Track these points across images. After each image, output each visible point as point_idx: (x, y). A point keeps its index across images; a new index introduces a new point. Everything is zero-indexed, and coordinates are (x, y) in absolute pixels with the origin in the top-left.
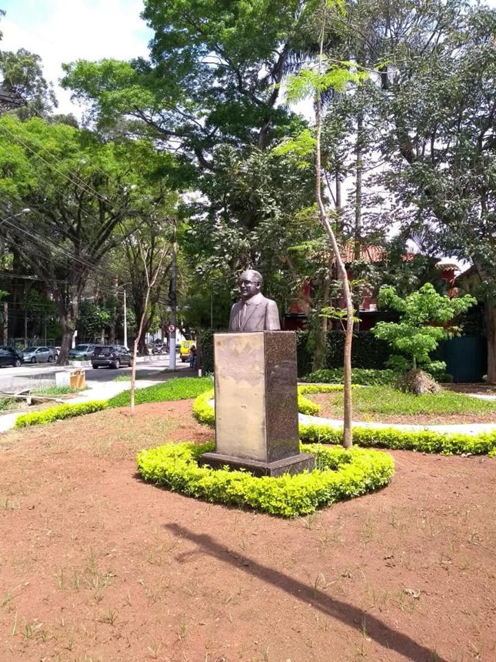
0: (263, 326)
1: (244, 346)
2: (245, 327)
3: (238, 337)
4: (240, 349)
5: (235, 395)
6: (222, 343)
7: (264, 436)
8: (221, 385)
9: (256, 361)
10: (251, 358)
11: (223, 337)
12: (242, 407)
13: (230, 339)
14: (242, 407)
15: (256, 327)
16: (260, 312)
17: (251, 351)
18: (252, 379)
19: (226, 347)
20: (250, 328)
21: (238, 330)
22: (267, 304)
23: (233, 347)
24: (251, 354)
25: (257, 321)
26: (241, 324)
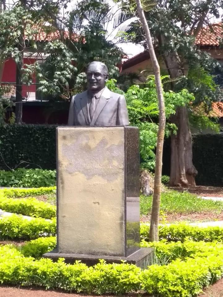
0: (115, 121)
1: (98, 142)
2: (97, 120)
3: (91, 131)
4: (93, 144)
5: (85, 191)
6: (69, 137)
7: (121, 231)
8: (66, 182)
9: (113, 157)
10: (108, 153)
11: (69, 131)
12: (95, 203)
13: (80, 133)
14: (95, 203)
15: (109, 122)
16: (112, 106)
17: (108, 146)
18: (108, 175)
19: (74, 141)
20: (103, 123)
21: (87, 124)
22: (119, 99)
23: (84, 142)
24: (108, 149)
25: (110, 115)
26: (91, 118)
